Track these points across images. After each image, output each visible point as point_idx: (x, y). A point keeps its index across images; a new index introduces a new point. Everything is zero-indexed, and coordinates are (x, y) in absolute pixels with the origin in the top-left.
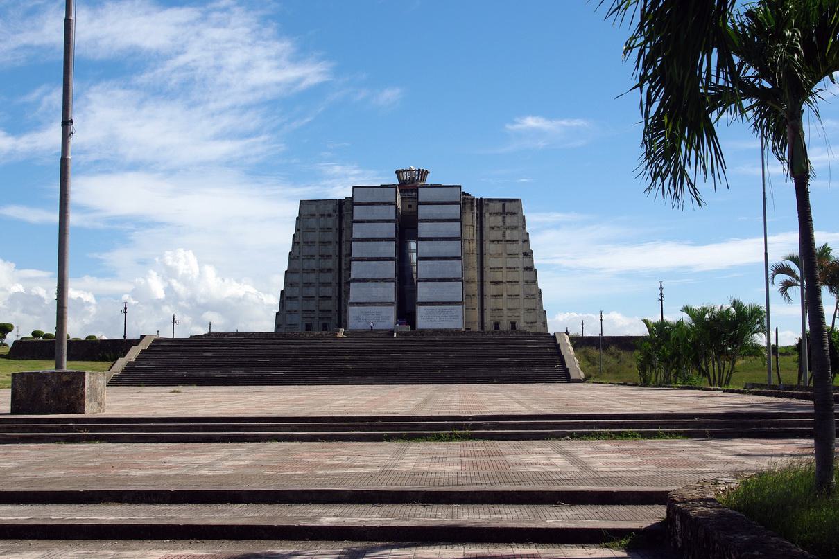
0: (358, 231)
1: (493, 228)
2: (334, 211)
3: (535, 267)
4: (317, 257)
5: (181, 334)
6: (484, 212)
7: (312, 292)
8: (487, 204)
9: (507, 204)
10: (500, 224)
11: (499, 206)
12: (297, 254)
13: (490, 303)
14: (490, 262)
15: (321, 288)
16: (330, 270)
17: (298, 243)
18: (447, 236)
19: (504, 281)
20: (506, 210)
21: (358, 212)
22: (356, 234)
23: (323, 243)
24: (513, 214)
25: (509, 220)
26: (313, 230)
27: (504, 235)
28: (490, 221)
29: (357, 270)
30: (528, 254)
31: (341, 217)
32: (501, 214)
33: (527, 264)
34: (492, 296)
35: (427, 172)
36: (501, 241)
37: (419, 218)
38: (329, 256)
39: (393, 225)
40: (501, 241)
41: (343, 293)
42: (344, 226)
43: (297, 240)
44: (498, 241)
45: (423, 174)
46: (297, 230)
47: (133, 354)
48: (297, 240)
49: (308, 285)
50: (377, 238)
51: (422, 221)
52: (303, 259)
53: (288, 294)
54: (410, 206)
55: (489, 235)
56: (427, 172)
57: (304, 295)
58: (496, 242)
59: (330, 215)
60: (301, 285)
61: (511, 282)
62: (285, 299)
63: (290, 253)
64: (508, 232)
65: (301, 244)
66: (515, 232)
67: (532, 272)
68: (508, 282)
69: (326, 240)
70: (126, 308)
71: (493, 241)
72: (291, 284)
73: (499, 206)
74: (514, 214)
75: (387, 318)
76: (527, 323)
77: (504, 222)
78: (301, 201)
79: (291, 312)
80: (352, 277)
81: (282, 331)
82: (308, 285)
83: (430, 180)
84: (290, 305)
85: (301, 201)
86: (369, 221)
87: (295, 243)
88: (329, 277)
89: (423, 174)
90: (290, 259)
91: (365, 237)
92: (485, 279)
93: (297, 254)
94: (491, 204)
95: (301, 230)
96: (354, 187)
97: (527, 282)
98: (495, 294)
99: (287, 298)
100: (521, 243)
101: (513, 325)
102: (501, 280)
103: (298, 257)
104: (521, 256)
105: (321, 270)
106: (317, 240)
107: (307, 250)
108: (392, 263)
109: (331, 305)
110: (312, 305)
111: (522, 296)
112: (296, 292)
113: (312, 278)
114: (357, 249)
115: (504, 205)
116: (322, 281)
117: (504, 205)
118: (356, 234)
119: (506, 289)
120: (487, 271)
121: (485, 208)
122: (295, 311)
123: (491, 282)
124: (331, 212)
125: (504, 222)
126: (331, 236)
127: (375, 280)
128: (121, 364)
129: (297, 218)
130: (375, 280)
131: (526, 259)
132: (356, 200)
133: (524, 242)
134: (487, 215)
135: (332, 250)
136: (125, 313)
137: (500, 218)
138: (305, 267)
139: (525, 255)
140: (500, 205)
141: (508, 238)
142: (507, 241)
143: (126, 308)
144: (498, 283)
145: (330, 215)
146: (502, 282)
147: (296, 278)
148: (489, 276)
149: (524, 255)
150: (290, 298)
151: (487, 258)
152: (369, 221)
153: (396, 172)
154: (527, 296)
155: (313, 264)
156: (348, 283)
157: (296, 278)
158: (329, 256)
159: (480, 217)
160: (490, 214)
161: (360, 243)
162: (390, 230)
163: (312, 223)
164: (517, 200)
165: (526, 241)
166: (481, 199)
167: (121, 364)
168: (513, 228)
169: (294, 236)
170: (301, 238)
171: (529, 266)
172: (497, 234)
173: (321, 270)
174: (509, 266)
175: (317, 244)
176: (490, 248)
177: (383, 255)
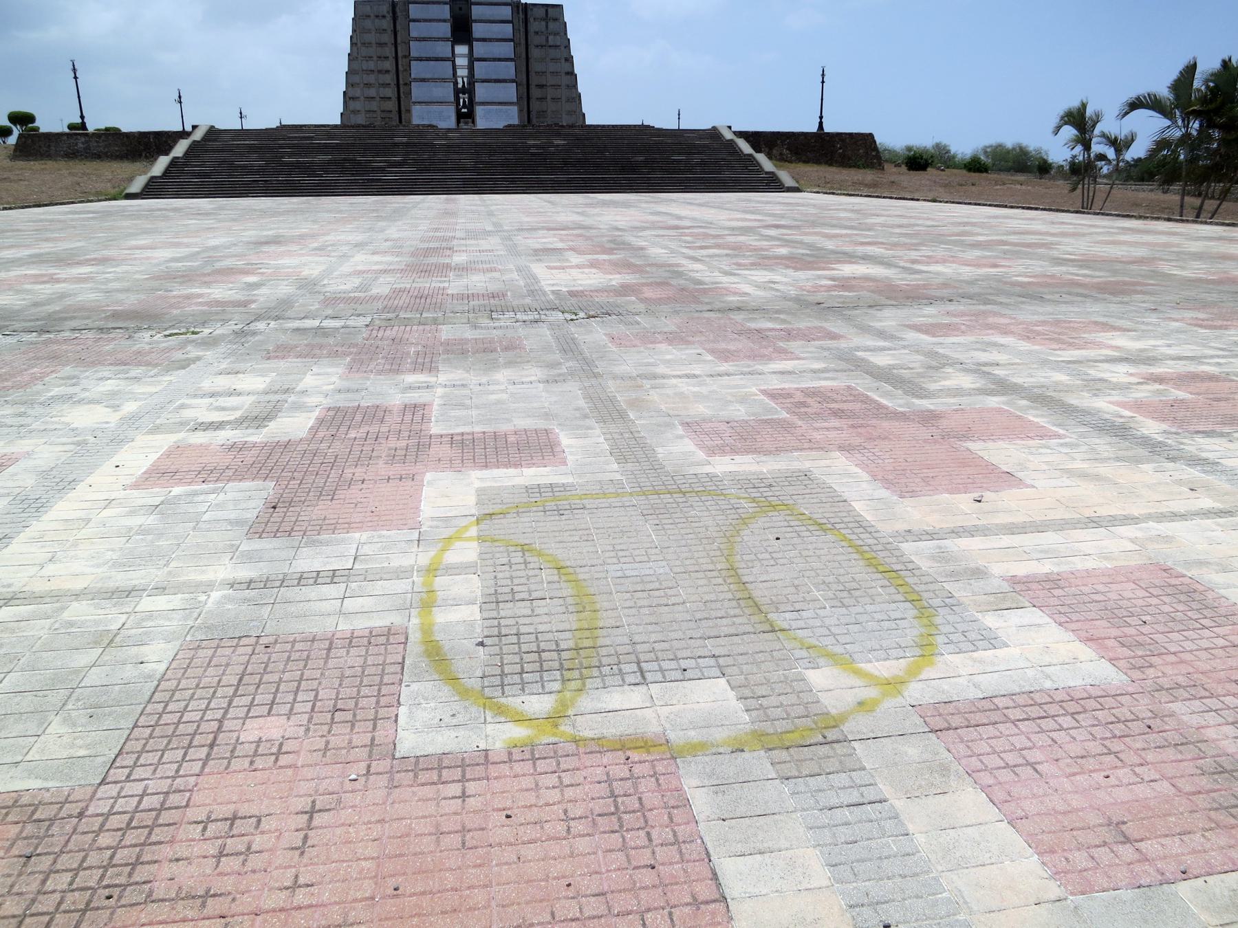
0: (416, 30)
1: (537, 33)
2: (388, 12)
3: (576, 71)
4: (375, 58)
5: (251, 124)
7: (372, 92)
9: (550, 10)
10: (544, 29)
11: (542, 12)
12: (355, 54)
13: (535, 106)
14: (536, 66)
15: (381, 89)
16: (387, 72)
22: (414, 34)
23: (380, 45)
24: (555, 20)
25: (552, 25)
26: (369, 31)
27: (547, 40)
28: (534, 26)
29: (417, 69)
30: (569, 60)
38: (386, 58)
39: (448, 25)
41: (402, 95)
42: (398, 27)
46: (354, 31)
47: (180, 149)
48: (354, 40)
49: (368, 85)
51: (476, 21)
54: (460, 9)
55: (535, 40)
59: (384, 17)
60: (362, 85)
64: (551, 38)
65: (359, 45)
66: (558, 37)
69: (382, 41)
70: (180, 97)
73: (542, 12)
75: (446, 119)
77: (547, 27)
79: (355, 112)
80: (413, 76)
82: (368, 85)
84: (354, 105)
86: (425, 21)
87: (353, 44)
88: (389, 78)
93: (355, 54)
94: (535, 9)
98: (540, 96)
100: (562, 48)
104: (563, 61)
105: (380, 72)
106: (374, 42)
107: (364, 51)
109: (391, 105)
110: (374, 106)
111: (564, 99)
112: (357, 92)
113: (371, 79)
114: (416, 49)
115: (547, 11)
116: (381, 82)
117: (547, 11)
119: (551, 93)
120: (532, 74)
121: (529, 13)
124: (385, 13)
125: (547, 27)
126: (387, 38)
128: (162, 163)
131: (568, 64)
134: (531, 20)
135: (389, 51)
136: (180, 102)
137: (543, 23)
138: (365, 68)
139: (567, 60)
140: (543, 10)
141: (551, 43)
143: (180, 97)
144: (541, 86)
145: (384, 17)
147: (356, 79)
148: (534, 80)
150: (353, 98)
151: (531, 61)
154: (568, 101)
155: (371, 65)
156: (408, 84)
157: (356, 79)
158: (386, 58)
162: (445, 29)
163: (368, 24)
165: (568, 46)
167: (162, 163)
168: (556, 34)
173: (380, 72)
175: (374, 46)
176: (535, 53)
177: (441, 55)
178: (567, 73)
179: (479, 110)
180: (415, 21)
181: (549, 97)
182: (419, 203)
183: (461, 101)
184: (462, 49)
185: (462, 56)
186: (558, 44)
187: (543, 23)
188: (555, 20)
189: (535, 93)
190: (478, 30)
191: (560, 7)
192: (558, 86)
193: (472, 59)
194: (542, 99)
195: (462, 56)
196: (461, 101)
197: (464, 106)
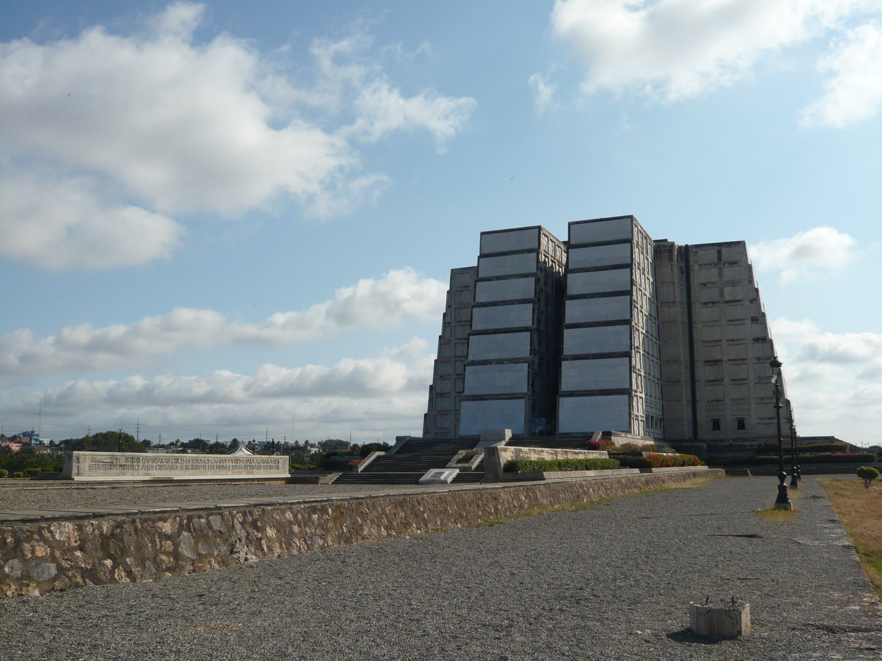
6: (691, 263)
8: (696, 252)
9: (724, 250)
11: (713, 254)
13: (704, 393)
14: (702, 333)
17: (450, 323)
18: (609, 290)
19: (725, 359)
20: (724, 259)
24: (733, 263)
25: (728, 272)
27: (722, 294)
28: (699, 276)
30: (760, 319)
32: (716, 264)
33: (757, 332)
34: (707, 381)
36: (718, 302)
40: (718, 302)
43: (448, 319)
44: (713, 303)
46: (448, 306)
48: (448, 319)
50: (507, 301)
52: (455, 344)
53: (439, 390)
55: (700, 295)
57: (457, 391)
58: (710, 305)
61: (735, 360)
62: (434, 395)
63: (440, 337)
64: (727, 290)
65: (453, 324)
67: (767, 345)
68: (730, 360)
71: (706, 304)
72: (441, 377)
73: (713, 254)
74: (735, 263)
76: (762, 419)
77: (720, 275)
78: (452, 271)
81: (430, 436)
85: (452, 271)
87: (446, 324)
90: (440, 345)
91: (492, 300)
92: (696, 357)
94: (701, 252)
95: (453, 306)
96: (483, 234)
97: (758, 359)
98: (712, 379)
99: (437, 394)
100: (747, 304)
101: (741, 424)
102: (719, 357)
103: (449, 341)
104: (749, 322)
108: (526, 335)
115: (719, 252)
117: (719, 252)
118: (480, 299)
120: (698, 346)
121: (692, 258)
122: (447, 411)
123: (705, 362)
125: (720, 275)
127: (500, 362)
129: (448, 292)
130: (500, 362)
133: (751, 301)
134: (696, 267)
137: (715, 271)
138: (459, 354)
139: (754, 320)
140: (714, 252)
142: (727, 302)
144: (716, 362)
146: (721, 361)
148: (701, 353)
149: (753, 320)
150: (441, 395)
151: (698, 328)
159: (687, 271)
160: (700, 265)
161: (484, 309)
164: (739, 243)
166: (687, 246)
168: (734, 283)
169: (445, 315)
170: (453, 317)
171: (761, 335)
172: (711, 294)
174: (730, 337)
176: (702, 314)
178: (757, 340)
181: (727, 380)
186: (739, 297)
187: (715, 271)
188: (733, 263)
189: (704, 373)
192: (738, 361)
194: (716, 382)
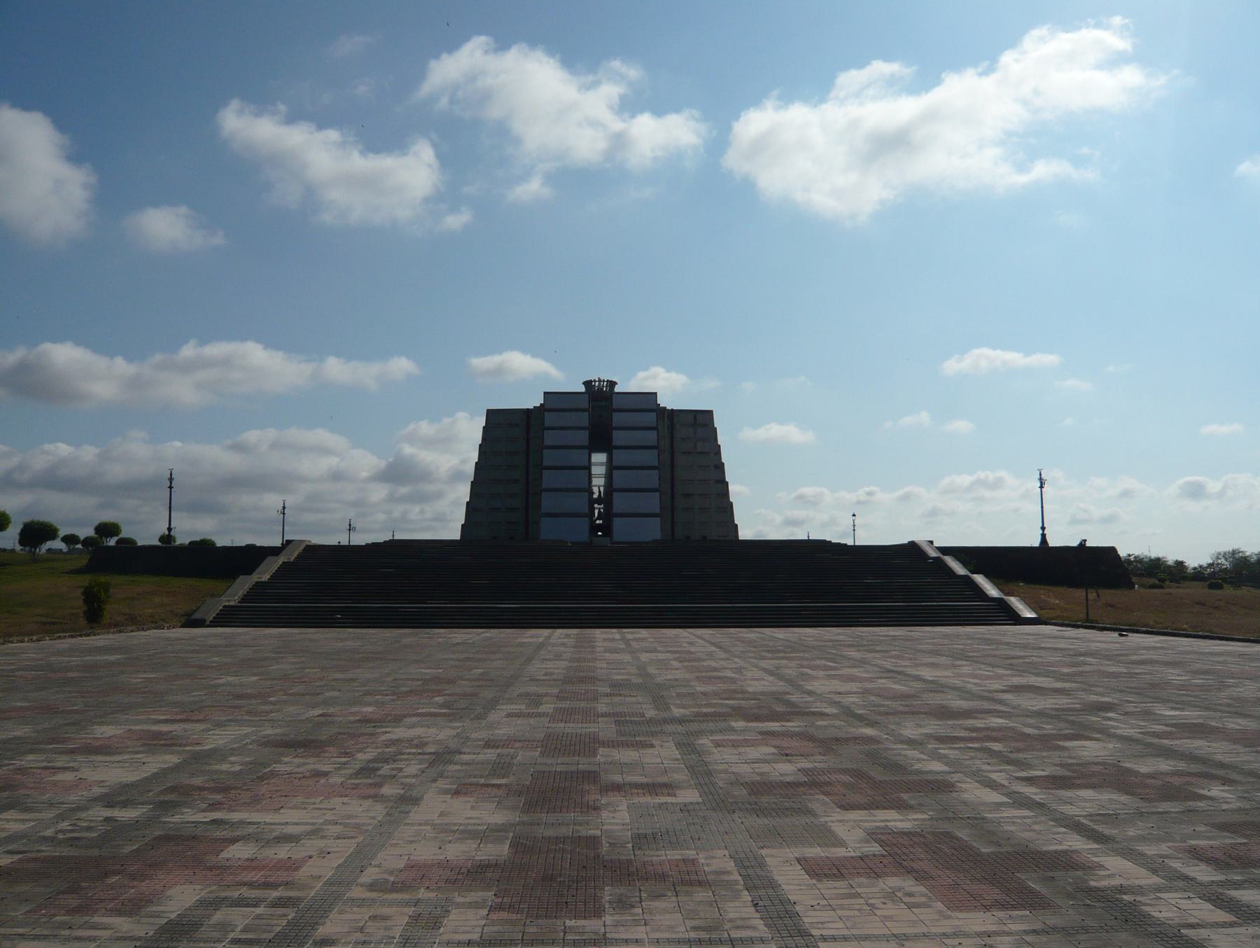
21: (549, 419)
22: (548, 442)
31: (528, 428)
35: (615, 383)
37: (614, 425)
39: (587, 432)
44: (689, 453)
45: (612, 384)
56: (615, 383)
71: (684, 453)
74: (706, 425)
83: (617, 389)
86: (562, 428)
89: (612, 384)
114: (549, 458)
115: (695, 417)
117: (695, 417)
118: (548, 442)
132: (547, 406)
142: (699, 453)
144: (688, 496)
152: (562, 428)
153: (584, 383)
162: (583, 437)
179: (617, 523)
180: (549, 429)
182: (541, 646)
183: (596, 512)
184: (599, 458)
185: (601, 464)
190: (619, 437)
191: (709, 414)
193: (611, 467)
195: (601, 464)
196: (596, 512)
197: (599, 518)
